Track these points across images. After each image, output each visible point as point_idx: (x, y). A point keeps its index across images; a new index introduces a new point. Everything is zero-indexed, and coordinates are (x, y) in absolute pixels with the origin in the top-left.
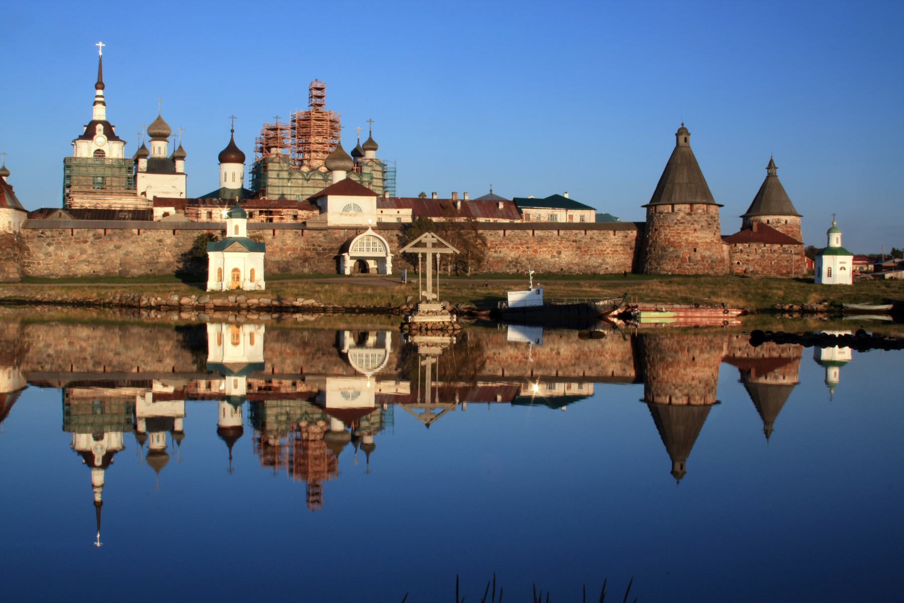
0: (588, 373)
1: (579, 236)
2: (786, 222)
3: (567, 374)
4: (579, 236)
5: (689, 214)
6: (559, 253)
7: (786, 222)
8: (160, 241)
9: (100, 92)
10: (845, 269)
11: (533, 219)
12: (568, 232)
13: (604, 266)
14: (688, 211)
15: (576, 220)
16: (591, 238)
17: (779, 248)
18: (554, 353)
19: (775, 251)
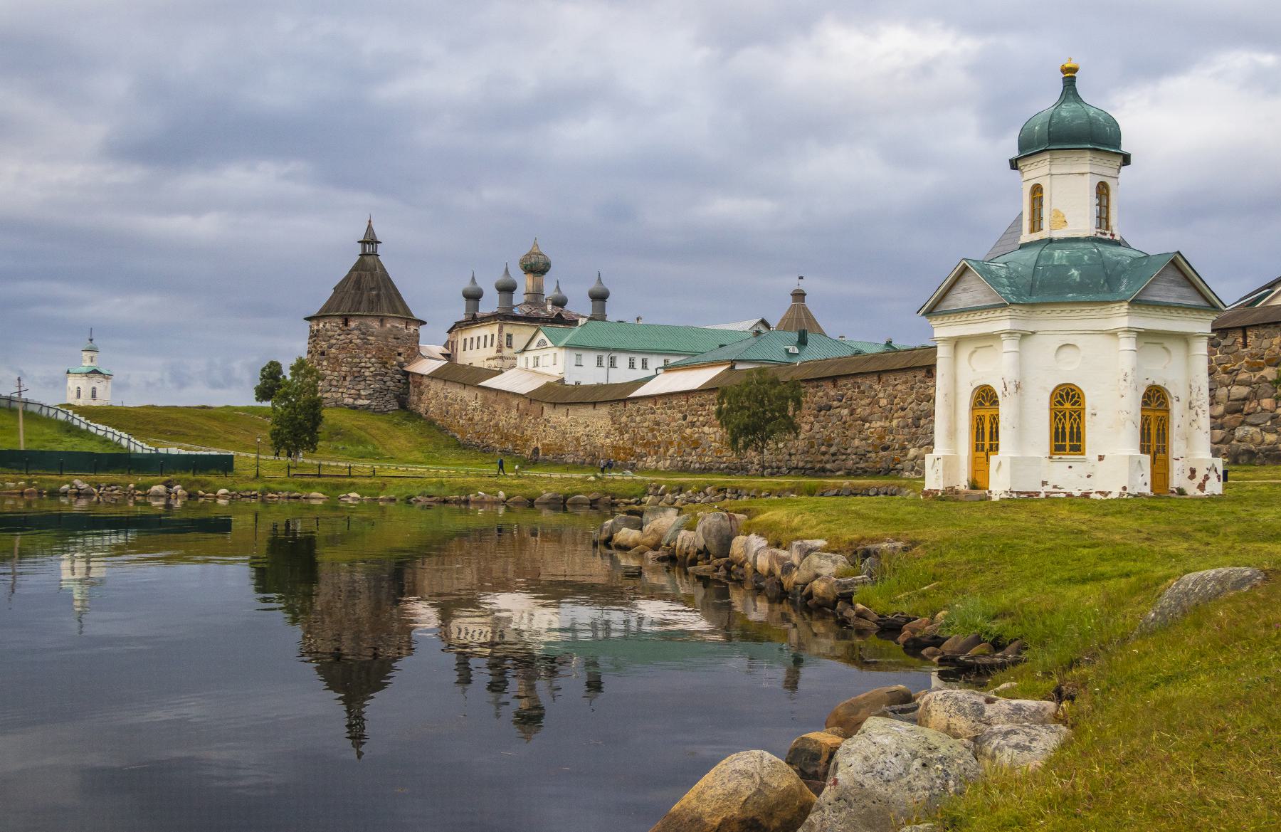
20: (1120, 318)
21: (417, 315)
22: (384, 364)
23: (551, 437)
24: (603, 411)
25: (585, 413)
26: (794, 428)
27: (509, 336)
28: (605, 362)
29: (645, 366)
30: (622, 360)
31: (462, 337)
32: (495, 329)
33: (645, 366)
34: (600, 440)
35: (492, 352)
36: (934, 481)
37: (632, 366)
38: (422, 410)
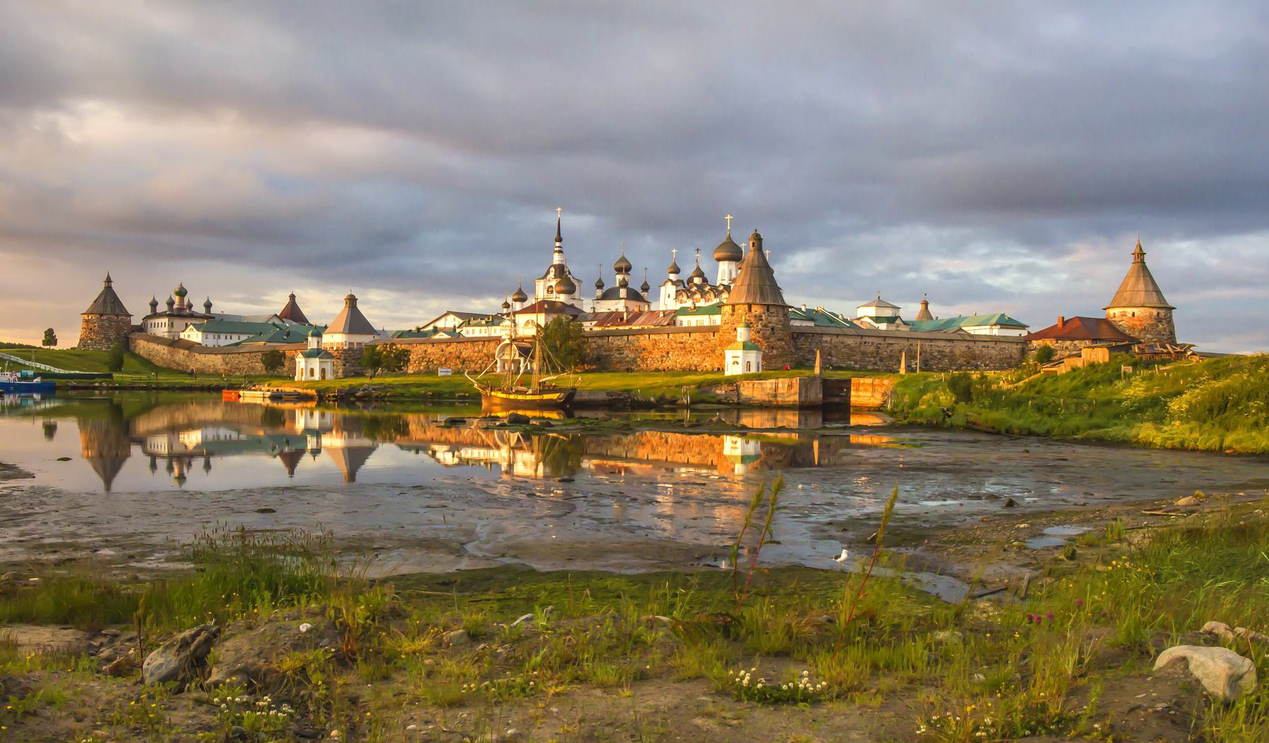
0: (691, 460)
1: (685, 338)
2: (1133, 314)
3: (675, 460)
4: (685, 338)
5: (732, 315)
6: (668, 353)
7: (1133, 314)
8: (426, 351)
9: (558, 244)
10: (737, 363)
11: (685, 325)
12: (676, 335)
13: (704, 364)
14: (730, 312)
15: (694, 324)
16: (695, 340)
17: (1070, 345)
18: (663, 441)
19: (1067, 348)
20: (317, 359)
21: (130, 313)
22: (118, 334)
23: (198, 365)
24: (220, 357)
25: (212, 357)
26: (283, 365)
27: (172, 323)
28: (216, 337)
29: (231, 338)
30: (223, 336)
31: (150, 321)
32: (165, 320)
33: (231, 338)
34: (219, 366)
35: (166, 329)
36: (296, 379)
37: (226, 338)
38: (137, 352)
